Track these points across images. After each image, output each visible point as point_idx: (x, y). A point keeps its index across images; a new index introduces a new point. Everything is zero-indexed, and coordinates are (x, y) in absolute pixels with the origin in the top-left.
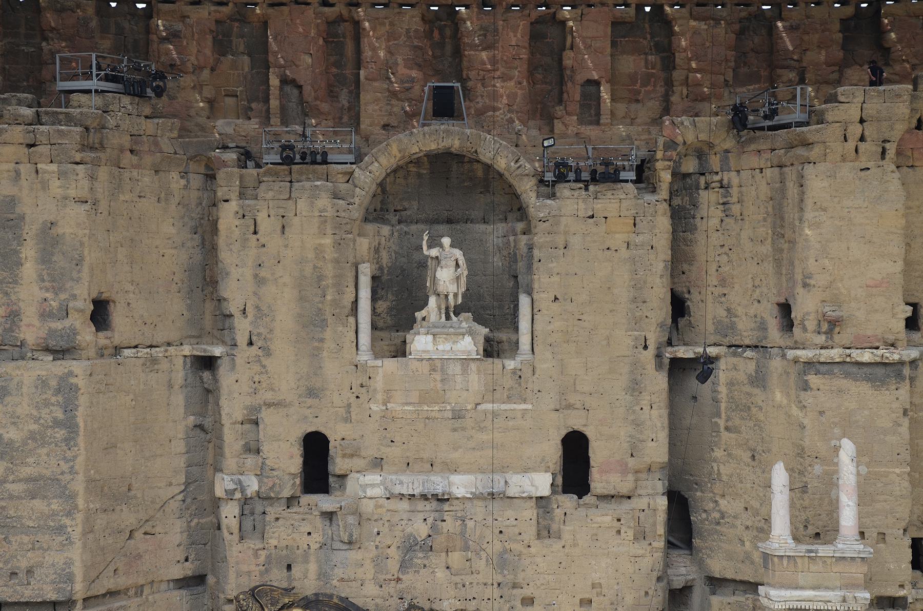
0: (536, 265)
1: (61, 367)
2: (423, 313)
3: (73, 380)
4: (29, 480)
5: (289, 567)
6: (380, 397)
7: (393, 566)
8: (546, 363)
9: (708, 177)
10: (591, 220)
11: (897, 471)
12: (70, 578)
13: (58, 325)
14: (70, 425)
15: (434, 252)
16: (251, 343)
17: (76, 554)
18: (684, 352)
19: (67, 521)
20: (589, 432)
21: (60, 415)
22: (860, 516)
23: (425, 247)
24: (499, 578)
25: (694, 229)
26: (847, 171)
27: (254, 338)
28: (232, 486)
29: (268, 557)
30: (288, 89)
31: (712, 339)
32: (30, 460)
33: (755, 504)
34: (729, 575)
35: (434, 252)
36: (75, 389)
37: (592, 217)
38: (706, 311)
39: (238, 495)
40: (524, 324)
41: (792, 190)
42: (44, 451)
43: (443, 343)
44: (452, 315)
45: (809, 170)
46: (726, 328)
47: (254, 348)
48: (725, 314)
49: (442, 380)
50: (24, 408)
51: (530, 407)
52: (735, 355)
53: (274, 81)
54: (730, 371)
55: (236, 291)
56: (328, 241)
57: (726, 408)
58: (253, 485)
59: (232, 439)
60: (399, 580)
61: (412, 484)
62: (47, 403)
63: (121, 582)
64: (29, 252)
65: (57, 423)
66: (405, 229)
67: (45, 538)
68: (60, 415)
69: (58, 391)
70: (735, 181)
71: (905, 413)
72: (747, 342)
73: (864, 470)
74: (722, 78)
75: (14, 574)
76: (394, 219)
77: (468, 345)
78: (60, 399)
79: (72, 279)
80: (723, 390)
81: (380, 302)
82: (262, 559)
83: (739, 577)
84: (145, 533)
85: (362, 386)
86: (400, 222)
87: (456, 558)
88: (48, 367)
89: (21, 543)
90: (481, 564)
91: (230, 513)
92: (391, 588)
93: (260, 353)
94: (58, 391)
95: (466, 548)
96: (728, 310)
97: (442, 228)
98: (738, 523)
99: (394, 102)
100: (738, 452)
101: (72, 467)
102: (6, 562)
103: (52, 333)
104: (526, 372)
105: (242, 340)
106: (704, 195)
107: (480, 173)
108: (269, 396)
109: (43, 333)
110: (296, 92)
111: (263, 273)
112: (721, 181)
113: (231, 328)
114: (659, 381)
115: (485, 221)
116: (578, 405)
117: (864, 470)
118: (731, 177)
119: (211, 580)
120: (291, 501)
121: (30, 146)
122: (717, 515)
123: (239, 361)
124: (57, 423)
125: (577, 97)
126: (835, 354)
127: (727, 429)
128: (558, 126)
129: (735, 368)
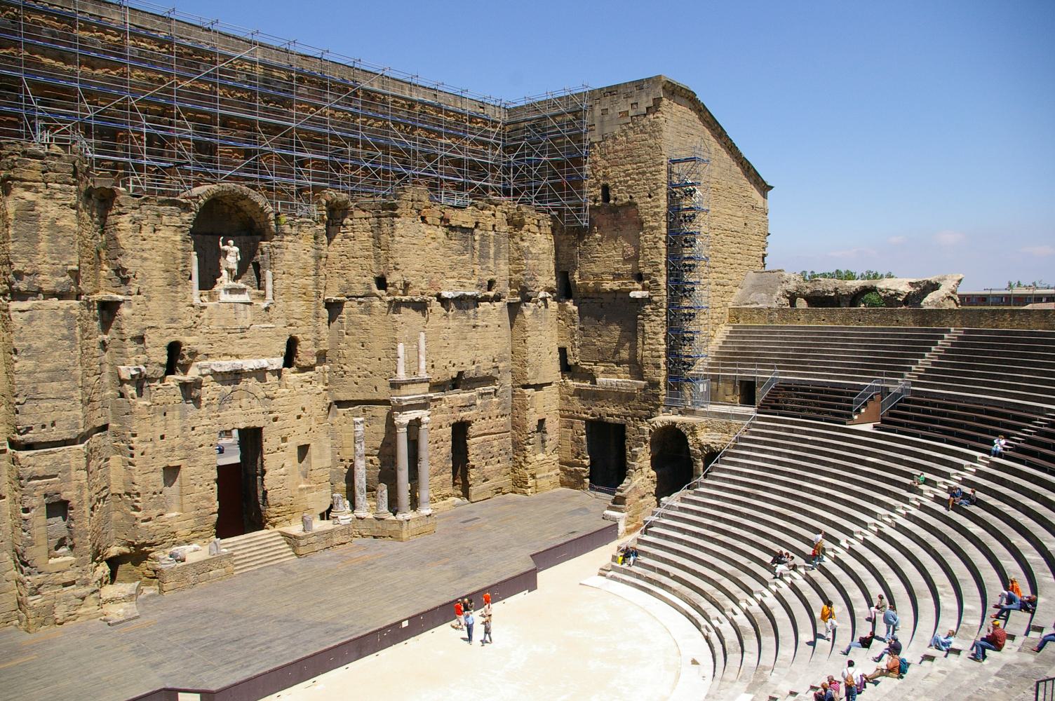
1: (65, 304)
2: (221, 278)
3: (73, 312)
4: (48, 371)
5: (165, 414)
6: (206, 322)
7: (215, 408)
8: (281, 304)
13: (62, 280)
15: (226, 247)
16: (139, 293)
17: (80, 413)
19: (73, 393)
20: (299, 336)
21: (65, 332)
23: (221, 243)
24: (264, 410)
26: (408, 221)
28: (134, 373)
29: (155, 409)
33: (365, 366)
34: (350, 398)
35: (226, 247)
36: (73, 316)
39: (137, 378)
40: (269, 286)
41: (386, 229)
42: (57, 353)
45: (396, 219)
50: (45, 329)
56: (178, 238)
60: (219, 416)
62: (57, 326)
64: (43, 234)
65: (65, 338)
67: (58, 403)
68: (65, 332)
69: (64, 318)
72: (359, 294)
75: (44, 426)
78: (65, 322)
79: (70, 253)
83: (355, 399)
85: (197, 316)
87: (244, 402)
88: (55, 302)
89: (47, 407)
92: (214, 420)
94: (64, 318)
95: (248, 397)
100: (355, 344)
101: (74, 362)
102: (39, 419)
103: (59, 284)
104: (272, 307)
105: (134, 290)
107: (226, 210)
108: (150, 324)
109: (53, 284)
114: (325, 312)
120: (162, 380)
121: (43, 172)
124: (65, 338)
126: (407, 298)
127: (347, 334)
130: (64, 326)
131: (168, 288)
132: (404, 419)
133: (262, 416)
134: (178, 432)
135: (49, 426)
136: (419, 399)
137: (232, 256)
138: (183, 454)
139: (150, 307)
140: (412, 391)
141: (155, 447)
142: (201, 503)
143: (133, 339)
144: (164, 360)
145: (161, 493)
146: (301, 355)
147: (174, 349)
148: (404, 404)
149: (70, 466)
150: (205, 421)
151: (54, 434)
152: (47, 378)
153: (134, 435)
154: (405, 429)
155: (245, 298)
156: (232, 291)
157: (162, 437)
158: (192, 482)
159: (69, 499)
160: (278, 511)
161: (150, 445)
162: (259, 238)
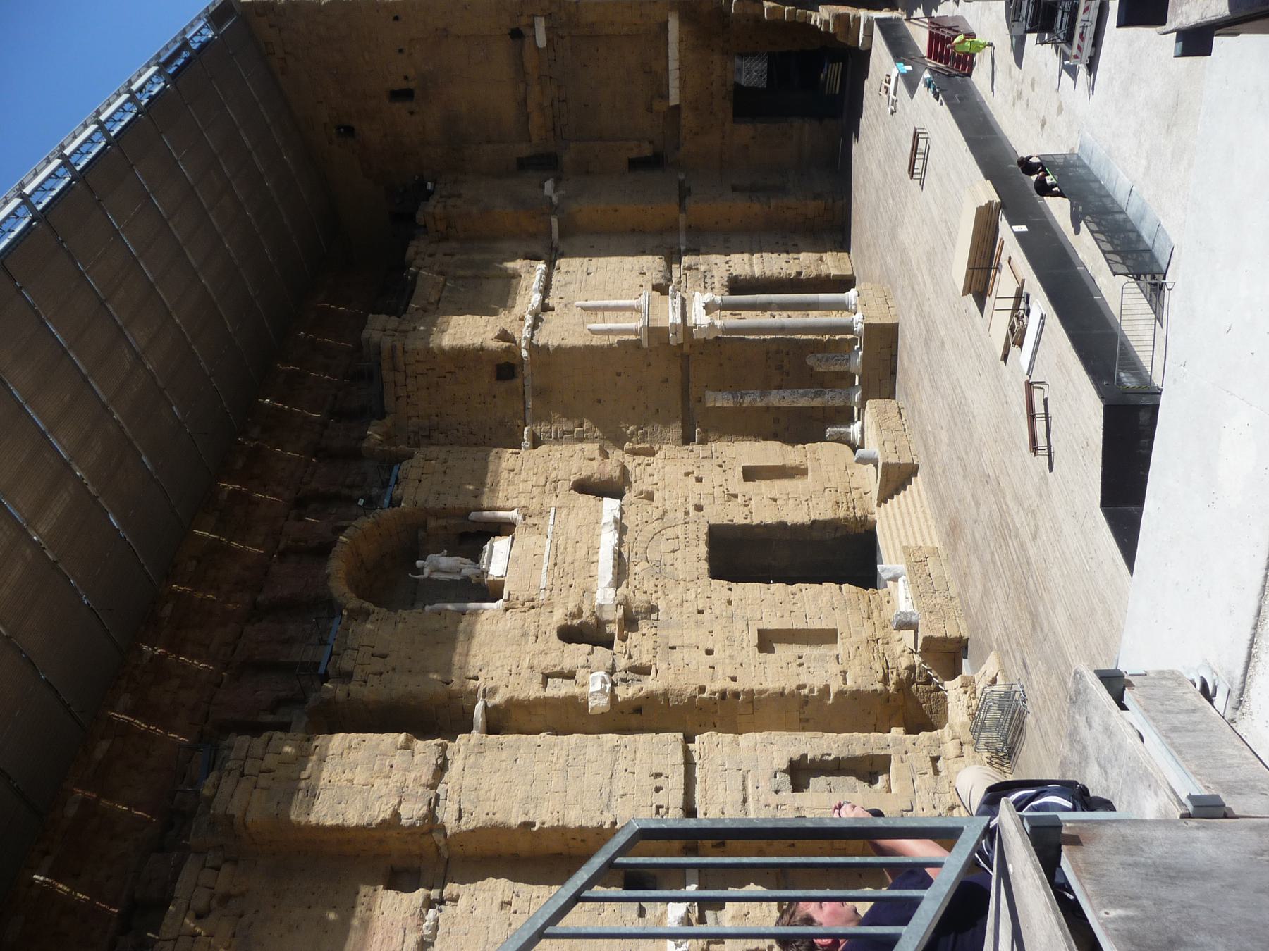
5: (673, 648)
15: (427, 572)
20: (573, 479)
43: (499, 558)
59: (559, 689)
90: (669, 533)
121: (242, 775)
123: (490, 684)
133: (692, 527)
135: (659, 782)
137: (441, 564)
141: (723, 664)
147: (569, 635)
153: (702, 689)
157: (709, 652)
160: (845, 508)
161: (719, 668)
162: (421, 534)
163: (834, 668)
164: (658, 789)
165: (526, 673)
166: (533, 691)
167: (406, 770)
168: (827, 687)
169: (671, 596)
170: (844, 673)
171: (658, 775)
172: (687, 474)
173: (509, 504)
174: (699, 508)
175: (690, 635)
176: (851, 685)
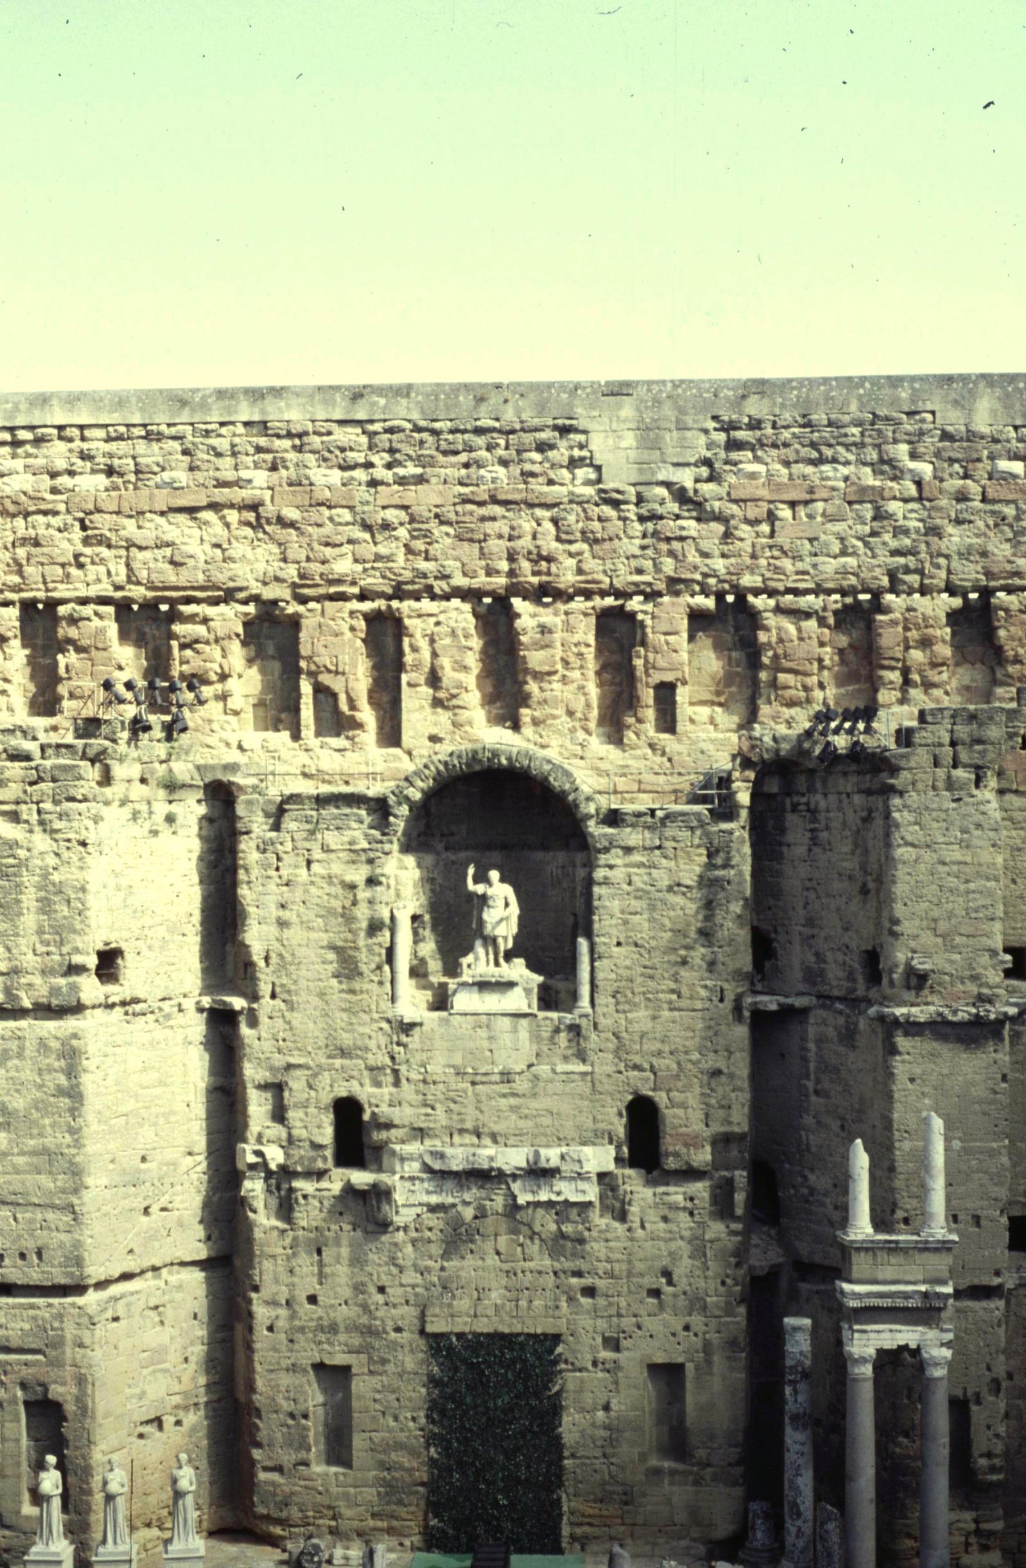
0: (596, 903)
4: (34, 1153)
5: (319, 1252)
7: (436, 1250)
9: (796, 799)
10: (657, 852)
11: (995, 1145)
12: (79, 1262)
14: (74, 1095)
15: (480, 889)
18: (770, 1003)
20: (661, 1098)
22: (948, 1199)
24: (557, 1266)
25: (779, 857)
27: (278, 990)
28: (251, 1159)
30: (321, 696)
31: (802, 987)
32: (35, 1131)
35: (480, 889)
37: (659, 847)
38: (795, 957)
42: (47, 1121)
44: (501, 960)
46: (813, 976)
47: (277, 1002)
48: (813, 959)
49: (490, 1038)
51: (589, 1069)
52: (823, 1007)
53: (306, 687)
54: (821, 1025)
55: (257, 937)
57: (817, 1068)
58: (275, 1156)
61: (457, 1157)
62: (50, 1070)
63: (131, 1265)
65: (61, 1092)
66: (453, 857)
70: (822, 804)
71: (1004, 1078)
72: (836, 993)
73: (957, 1144)
74: (815, 679)
76: (440, 846)
77: (517, 1000)
78: (63, 1063)
80: (812, 1046)
81: (421, 945)
82: (288, 1241)
84: (163, 1209)
86: (447, 849)
90: (534, 1248)
91: (254, 1187)
93: (283, 1006)
96: (817, 955)
97: (496, 856)
98: (828, 1201)
99: (439, 710)
106: (792, 820)
110: (330, 700)
111: (286, 915)
112: (808, 804)
113: (254, 980)
115: (545, 848)
116: (647, 1066)
117: (957, 1144)
118: (819, 800)
119: (237, 1262)
122: (805, 1191)
124: (61, 1092)
125: (651, 701)
127: (816, 1092)
128: (630, 736)
129: (824, 1023)
130: (62, 1070)
131: (334, 982)
132: (866, 1343)
134: (347, 1292)
136: (906, 1296)
138: (356, 1341)
139: (294, 1022)
140: (888, 1273)
142: (393, 1456)
143: (264, 1087)
144: (326, 1134)
145: (305, 1416)
146: (669, 1143)
147: (347, 1112)
148: (853, 1304)
149: (63, 1337)
150: (411, 1277)
151: (34, 1275)
152: (28, 1164)
154: (868, 1370)
155: (517, 1000)
156: (483, 986)
157: (312, 1299)
158: (378, 1407)
159: (60, 1399)
161: (283, 1312)
163: (287, 1457)
164: (23, 1256)
165: (279, 1060)
166: (252, 1072)
167: (43, 972)
168: (259, 1445)
169: (409, 1249)
170: (279, 1469)
171: (39, 1254)
172: (667, 1274)
173: (600, 1000)
174: (590, 1292)
175: (342, 1273)
176: (262, 1476)
